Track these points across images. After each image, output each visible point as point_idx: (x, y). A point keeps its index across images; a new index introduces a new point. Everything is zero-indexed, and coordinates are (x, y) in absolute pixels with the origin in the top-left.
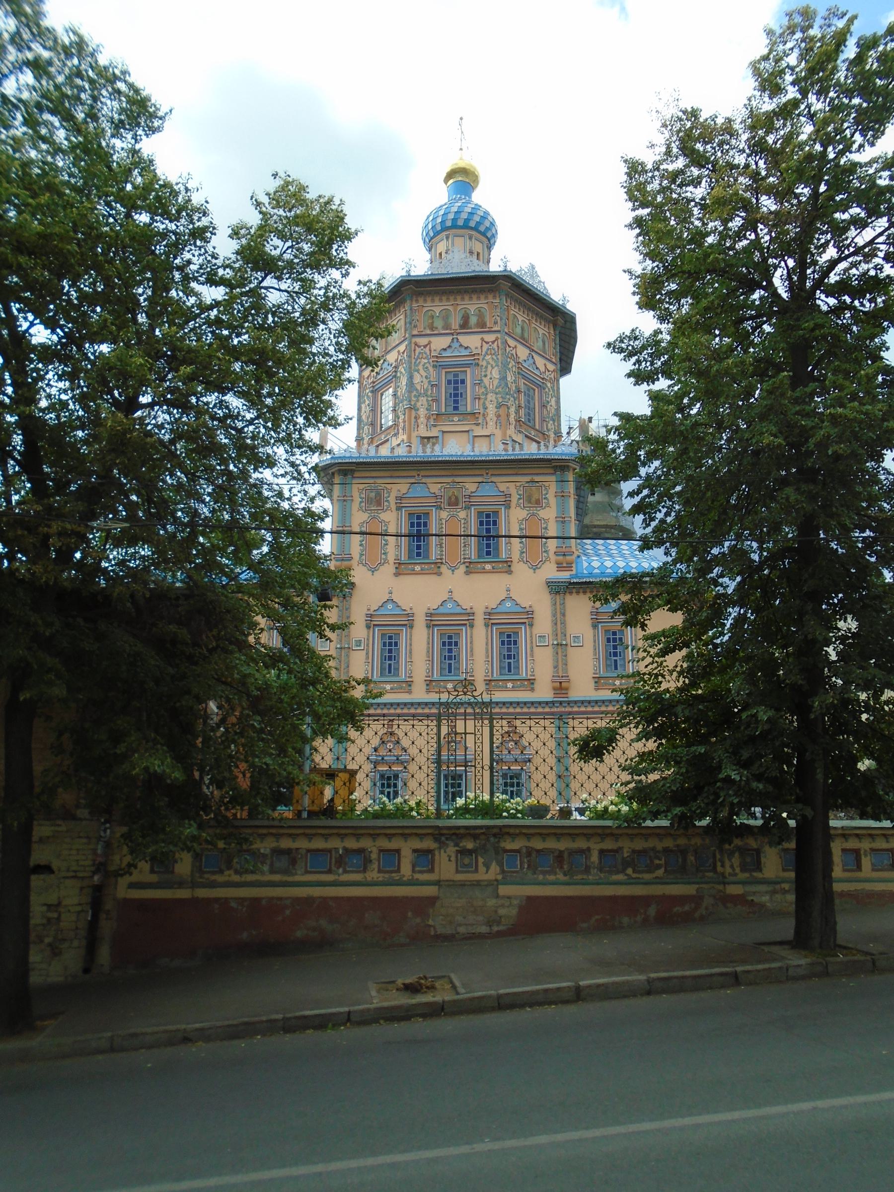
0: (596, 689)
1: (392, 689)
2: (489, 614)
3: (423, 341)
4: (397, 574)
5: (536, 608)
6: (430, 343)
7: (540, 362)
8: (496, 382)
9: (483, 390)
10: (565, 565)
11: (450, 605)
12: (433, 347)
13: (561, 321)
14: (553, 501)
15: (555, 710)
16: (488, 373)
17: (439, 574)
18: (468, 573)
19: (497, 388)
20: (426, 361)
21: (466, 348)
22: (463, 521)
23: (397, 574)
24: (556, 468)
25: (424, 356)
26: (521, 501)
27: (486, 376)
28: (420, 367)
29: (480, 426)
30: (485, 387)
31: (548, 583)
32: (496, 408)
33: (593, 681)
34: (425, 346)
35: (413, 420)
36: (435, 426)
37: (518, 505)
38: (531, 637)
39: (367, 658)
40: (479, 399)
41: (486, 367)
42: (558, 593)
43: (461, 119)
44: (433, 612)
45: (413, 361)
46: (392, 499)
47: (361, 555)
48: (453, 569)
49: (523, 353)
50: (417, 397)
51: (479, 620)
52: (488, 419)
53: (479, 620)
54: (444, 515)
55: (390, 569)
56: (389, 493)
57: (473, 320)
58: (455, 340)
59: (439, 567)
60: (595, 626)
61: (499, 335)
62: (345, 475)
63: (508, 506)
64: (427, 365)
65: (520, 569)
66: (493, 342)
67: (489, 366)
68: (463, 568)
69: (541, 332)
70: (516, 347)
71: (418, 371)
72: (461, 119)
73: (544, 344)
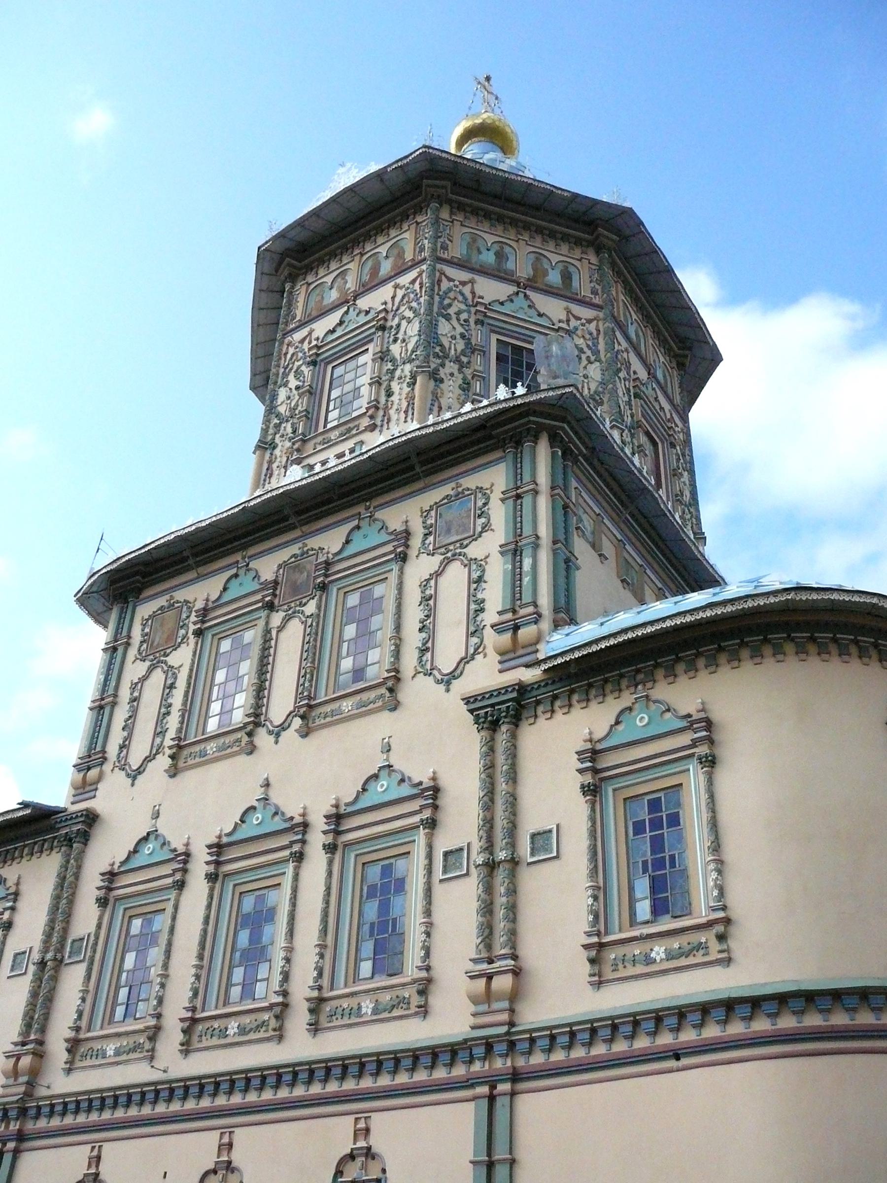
0: (599, 982)
1: (118, 1053)
2: (337, 818)
3: (298, 336)
4: (174, 772)
5: (444, 782)
6: (310, 334)
7: (554, 309)
8: (410, 347)
9: (390, 366)
10: (521, 652)
11: (256, 818)
12: (314, 335)
13: (608, 237)
14: (499, 513)
15: (477, 1067)
16: (400, 336)
17: (252, 749)
18: (305, 733)
19: (413, 352)
20: (301, 362)
21: (367, 312)
22: (309, 621)
23: (174, 772)
24: (499, 444)
25: (300, 355)
26: (431, 538)
27: (395, 341)
28: (291, 377)
29: (377, 431)
30: (393, 360)
31: (467, 700)
32: (409, 385)
33: (584, 955)
34: (302, 341)
35: (265, 466)
36: (298, 461)
37: (425, 550)
38: (430, 856)
39: (88, 977)
40: (380, 384)
41: (399, 326)
42: (494, 726)
43: (488, 79)
44: (225, 840)
45: (282, 370)
46: (193, 618)
47: (122, 747)
48: (277, 733)
49: (491, 290)
50: (278, 426)
51: (317, 839)
52: (392, 412)
53: (317, 839)
54: (277, 619)
55: (163, 761)
56: (190, 609)
57: (386, 267)
58: (351, 309)
59: (250, 734)
60: (592, 791)
61: (424, 267)
62: (126, 602)
63: (403, 558)
64: (303, 368)
65: (418, 691)
66: (413, 282)
67: (404, 323)
68: (297, 722)
69: (555, 258)
70: (472, 282)
71: (286, 385)
72: (488, 79)
73: (567, 277)
